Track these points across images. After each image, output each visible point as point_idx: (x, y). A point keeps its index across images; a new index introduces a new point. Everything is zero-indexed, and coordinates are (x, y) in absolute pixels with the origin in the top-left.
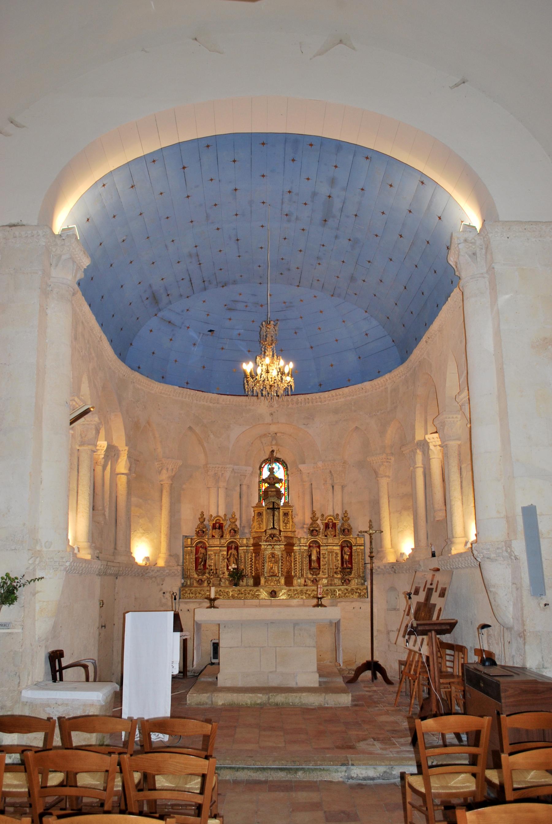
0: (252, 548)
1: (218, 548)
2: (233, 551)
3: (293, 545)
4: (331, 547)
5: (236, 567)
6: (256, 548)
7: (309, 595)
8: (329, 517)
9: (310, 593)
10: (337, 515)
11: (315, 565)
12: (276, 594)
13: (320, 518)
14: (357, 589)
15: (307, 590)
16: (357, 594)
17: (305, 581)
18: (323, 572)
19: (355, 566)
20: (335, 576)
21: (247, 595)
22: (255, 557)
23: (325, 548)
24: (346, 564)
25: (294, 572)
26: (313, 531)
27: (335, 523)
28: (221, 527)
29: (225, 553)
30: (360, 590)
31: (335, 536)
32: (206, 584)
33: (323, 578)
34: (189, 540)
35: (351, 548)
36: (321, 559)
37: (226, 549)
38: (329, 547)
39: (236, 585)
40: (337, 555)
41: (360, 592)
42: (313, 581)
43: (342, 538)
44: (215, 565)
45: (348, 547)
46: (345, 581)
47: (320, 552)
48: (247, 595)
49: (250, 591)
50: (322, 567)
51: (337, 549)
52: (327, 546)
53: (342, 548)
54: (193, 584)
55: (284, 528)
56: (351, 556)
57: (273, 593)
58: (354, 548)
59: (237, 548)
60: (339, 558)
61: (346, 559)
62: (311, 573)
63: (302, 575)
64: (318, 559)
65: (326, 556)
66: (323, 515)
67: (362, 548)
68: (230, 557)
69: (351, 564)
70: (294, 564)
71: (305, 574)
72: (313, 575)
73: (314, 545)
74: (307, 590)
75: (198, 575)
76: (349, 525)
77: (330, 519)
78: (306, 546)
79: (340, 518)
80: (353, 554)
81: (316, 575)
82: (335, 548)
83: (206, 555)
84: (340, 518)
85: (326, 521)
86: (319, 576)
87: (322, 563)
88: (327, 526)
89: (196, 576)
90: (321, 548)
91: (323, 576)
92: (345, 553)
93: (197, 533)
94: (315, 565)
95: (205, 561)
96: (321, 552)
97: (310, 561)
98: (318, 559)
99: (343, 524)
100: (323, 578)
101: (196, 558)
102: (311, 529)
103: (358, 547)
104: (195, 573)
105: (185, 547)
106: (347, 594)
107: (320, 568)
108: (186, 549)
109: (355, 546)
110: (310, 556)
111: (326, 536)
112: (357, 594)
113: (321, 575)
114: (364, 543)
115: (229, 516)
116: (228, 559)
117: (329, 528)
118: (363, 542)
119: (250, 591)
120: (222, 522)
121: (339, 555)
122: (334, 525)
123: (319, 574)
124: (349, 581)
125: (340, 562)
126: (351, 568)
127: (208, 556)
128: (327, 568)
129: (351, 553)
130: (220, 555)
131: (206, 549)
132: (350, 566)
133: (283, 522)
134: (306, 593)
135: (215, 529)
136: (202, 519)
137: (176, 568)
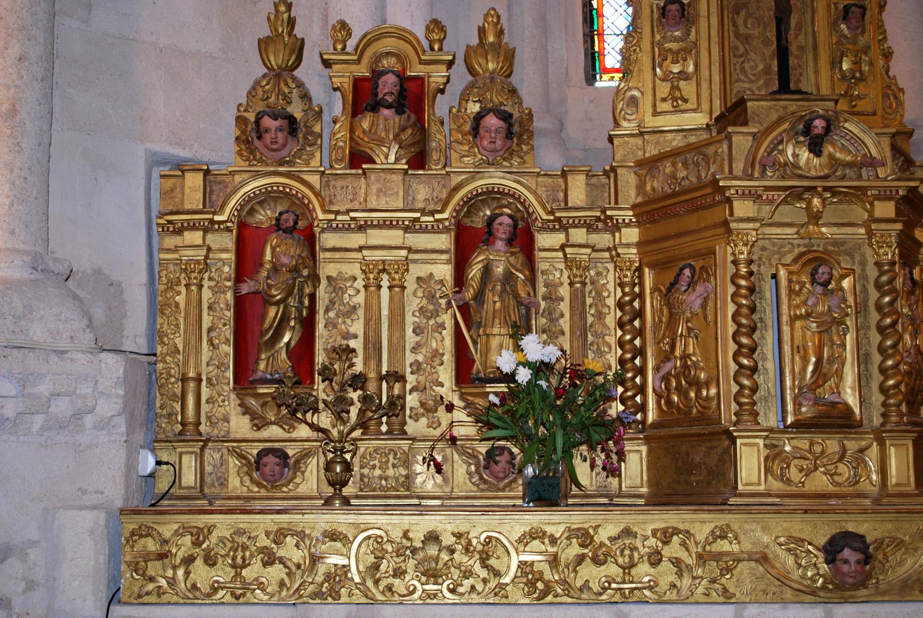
0: (632, 235)
1: (394, 236)
2: (498, 258)
5: (551, 353)
6: (658, 230)
12: (868, 559)
21: (644, 571)
22: (667, 293)
28: (412, 97)
29: (444, 271)
32: (311, 479)
34: (194, 181)
37: (444, 241)
39: (547, 493)
44: (373, 347)
48: (644, 571)
49: (666, 536)
54: (223, 483)
59: (523, 239)
68: (479, 297)
75: (259, 423)
83: (315, 278)
89: (240, 426)
93: (250, 136)
95: (308, 325)
101: (240, 303)
104: (232, 405)
105: (169, 223)
108: (171, 241)
115: (461, 37)
116: (464, 309)
119: (666, 536)
120: (415, 70)
127: (323, 293)
130: (411, 284)
131: (310, 239)
133: (835, 64)
135: (375, 107)
136: (283, 46)
137: (82, 362)
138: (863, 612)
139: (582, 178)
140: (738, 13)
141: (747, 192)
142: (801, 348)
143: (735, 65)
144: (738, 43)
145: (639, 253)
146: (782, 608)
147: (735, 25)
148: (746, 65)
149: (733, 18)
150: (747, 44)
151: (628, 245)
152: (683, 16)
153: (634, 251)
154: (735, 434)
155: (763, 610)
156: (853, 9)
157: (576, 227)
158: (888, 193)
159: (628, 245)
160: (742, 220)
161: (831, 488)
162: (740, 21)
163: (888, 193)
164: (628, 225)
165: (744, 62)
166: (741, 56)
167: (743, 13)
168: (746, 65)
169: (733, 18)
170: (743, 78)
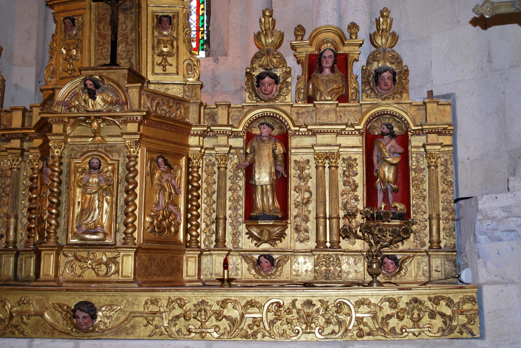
3: (184, 129)
4: (329, 143)
7: (233, 322)
8: (321, 36)
9: (235, 314)
10: (353, 26)
11: (266, 201)
13: (289, 38)
14: (436, 300)
15: (224, 303)
16: (438, 322)
17: (226, 265)
18: (297, 229)
19: (420, 208)
20: (344, 244)
23: (308, 141)
24: (386, 199)
25: (187, 231)
26: (260, 77)
27: (346, 56)
30: (450, 303)
31: (343, 98)
33: (295, 253)
35: (404, 141)
36: (293, 182)
38: (321, 139)
40: (350, 166)
41: (448, 312)
42: (259, 262)
43: (371, 104)
45: (392, 135)
46: (381, 264)
47: (286, 156)
50: (293, 211)
51: (352, 146)
52: (314, 133)
53: (370, 142)
55: (159, 69)
56: (403, 169)
57: (81, 314)
58: (416, 141)
60: (360, 179)
61: (384, 181)
62: (251, 235)
63: (220, 243)
64: (281, 185)
65: (311, 170)
66: (300, 31)
67: (447, 140)
69: (406, 200)
70: (188, 201)
71: (229, 238)
72: (259, 240)
73: (266, 130)
74: (224, 303)
76: (397, 60)
77: (325, 41)
78: (236, 135)
79: (363, 34)
80: (413, 163)
81: (272, 241)
82: (342, 140)
84: (363, 34)
85: (312, 50)
86: (280, 245)
87: (294, 196)
88: (313, 65)
90: (294, 142)
91: (299, 246)
92: (383, 159)
94: (266, 201)
96: (293, 158)
97: (250, 188)
98: (281, 185)
99: (372, 58)
100: (295, 253)
102: (256, 73)
103: (432, 138)
106: (393, 322)
107: (285, 217)
109: (417, 133)
110: (249, 172)
111: (310, 99)
112: (438, 322)
113: (290, 240)
114: (454, 124)
117: (321, 71)
118: (449, 120)
121: (360, 169)
122: (342, 63)
123: (281, 236)
124: (398, 264)
125: (361, 192)
126: (405, 216)
128: (312, 216)
129: (405, 156)
132: (400, 207)
134: (219, 316)
138: (95, 345)
139: (20, 113)
140: (100, 23)
141: (57, 120)
142: (80, 204)
143: (97, 51)
144: (100, 39)
145: (40, 152)
146: (53, 341)
147: (99, 29)
148: (104, 51)
149: (98, 26)
150: (104, 39)
151: (34, 148)
152: (74, 25)
153: (38, 151)
154: (40, 248)
155: (43, 342)
156: (163, 18)
157: (14, 139)
158: (132, 119)
159: (34, 148)
160: (56, 135)
161: (95, 278)
162: (101, 27)
163: (132, 119)
164: (36, 138)
165: (102, 49)
166: (101, 46)
167: (103, 23)
168: (104, 51)
169: (98, 26)
170: (101, 57)
